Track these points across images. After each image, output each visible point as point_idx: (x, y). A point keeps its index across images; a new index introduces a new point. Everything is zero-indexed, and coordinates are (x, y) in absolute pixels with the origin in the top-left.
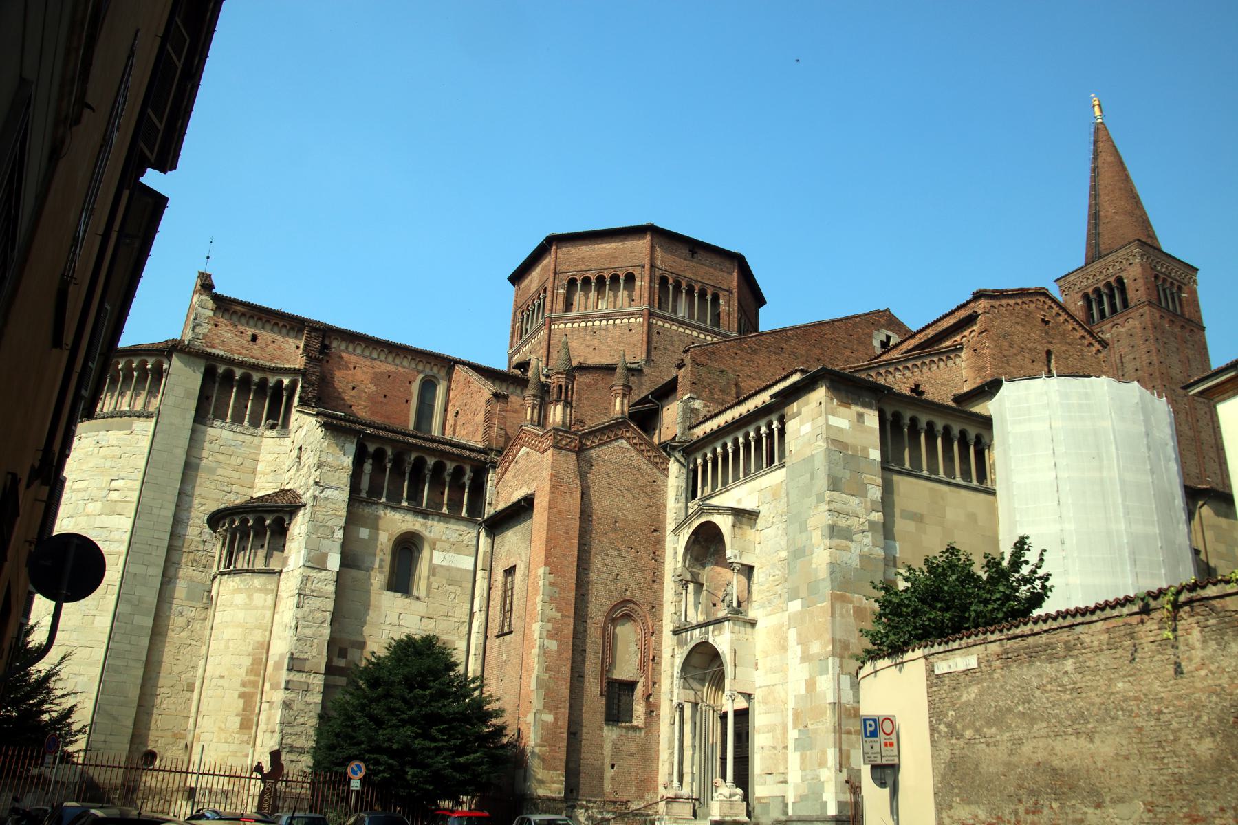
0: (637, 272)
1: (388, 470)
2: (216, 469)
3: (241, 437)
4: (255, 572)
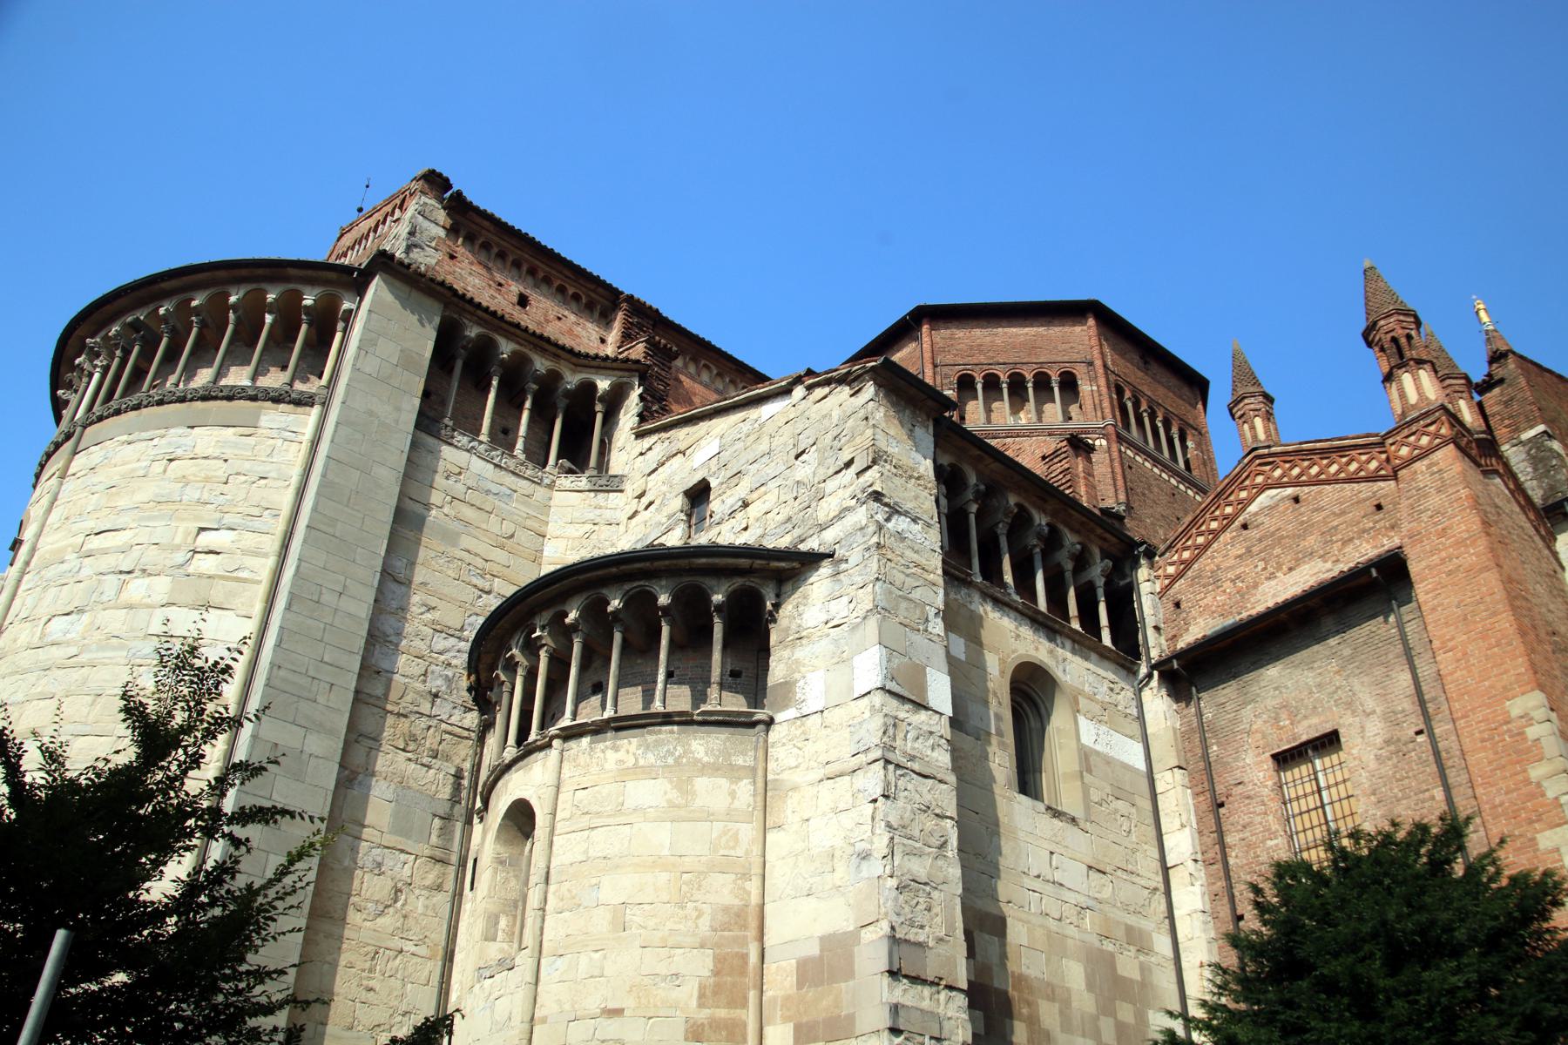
0: (1080, 372)
1: (972, 518)
2: (458, 535)
3: (510, 480)
4: (691, 723)
